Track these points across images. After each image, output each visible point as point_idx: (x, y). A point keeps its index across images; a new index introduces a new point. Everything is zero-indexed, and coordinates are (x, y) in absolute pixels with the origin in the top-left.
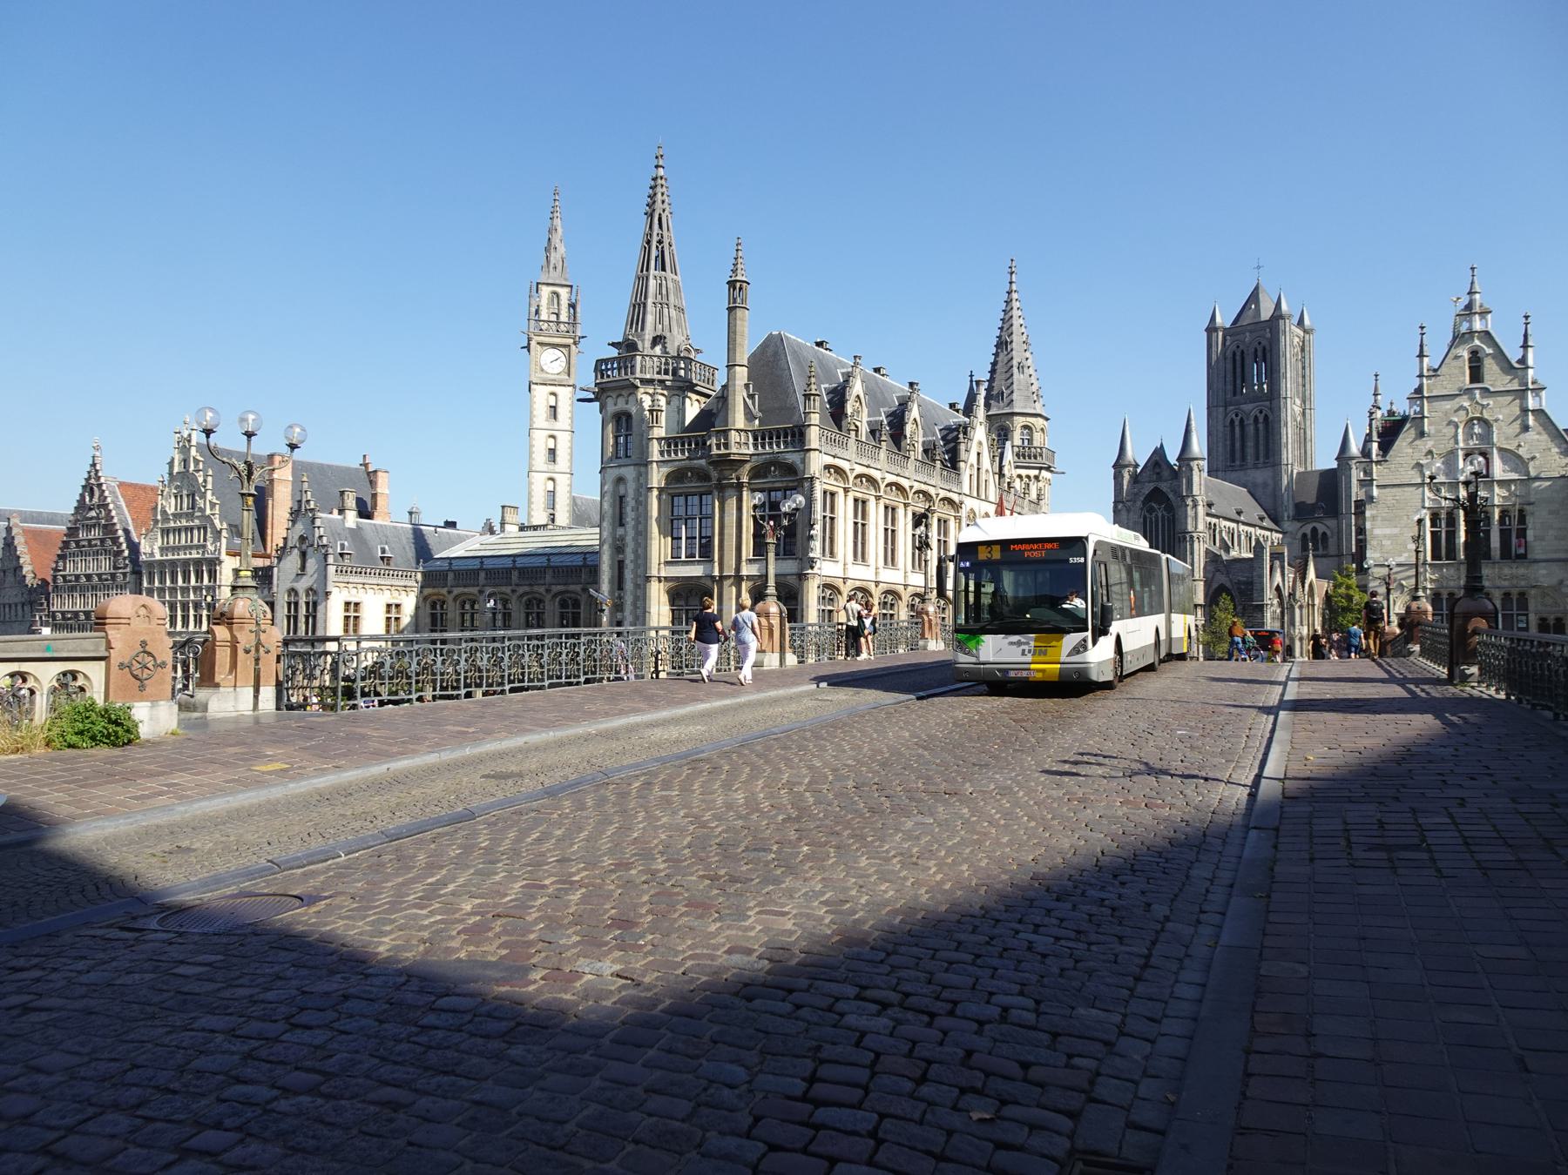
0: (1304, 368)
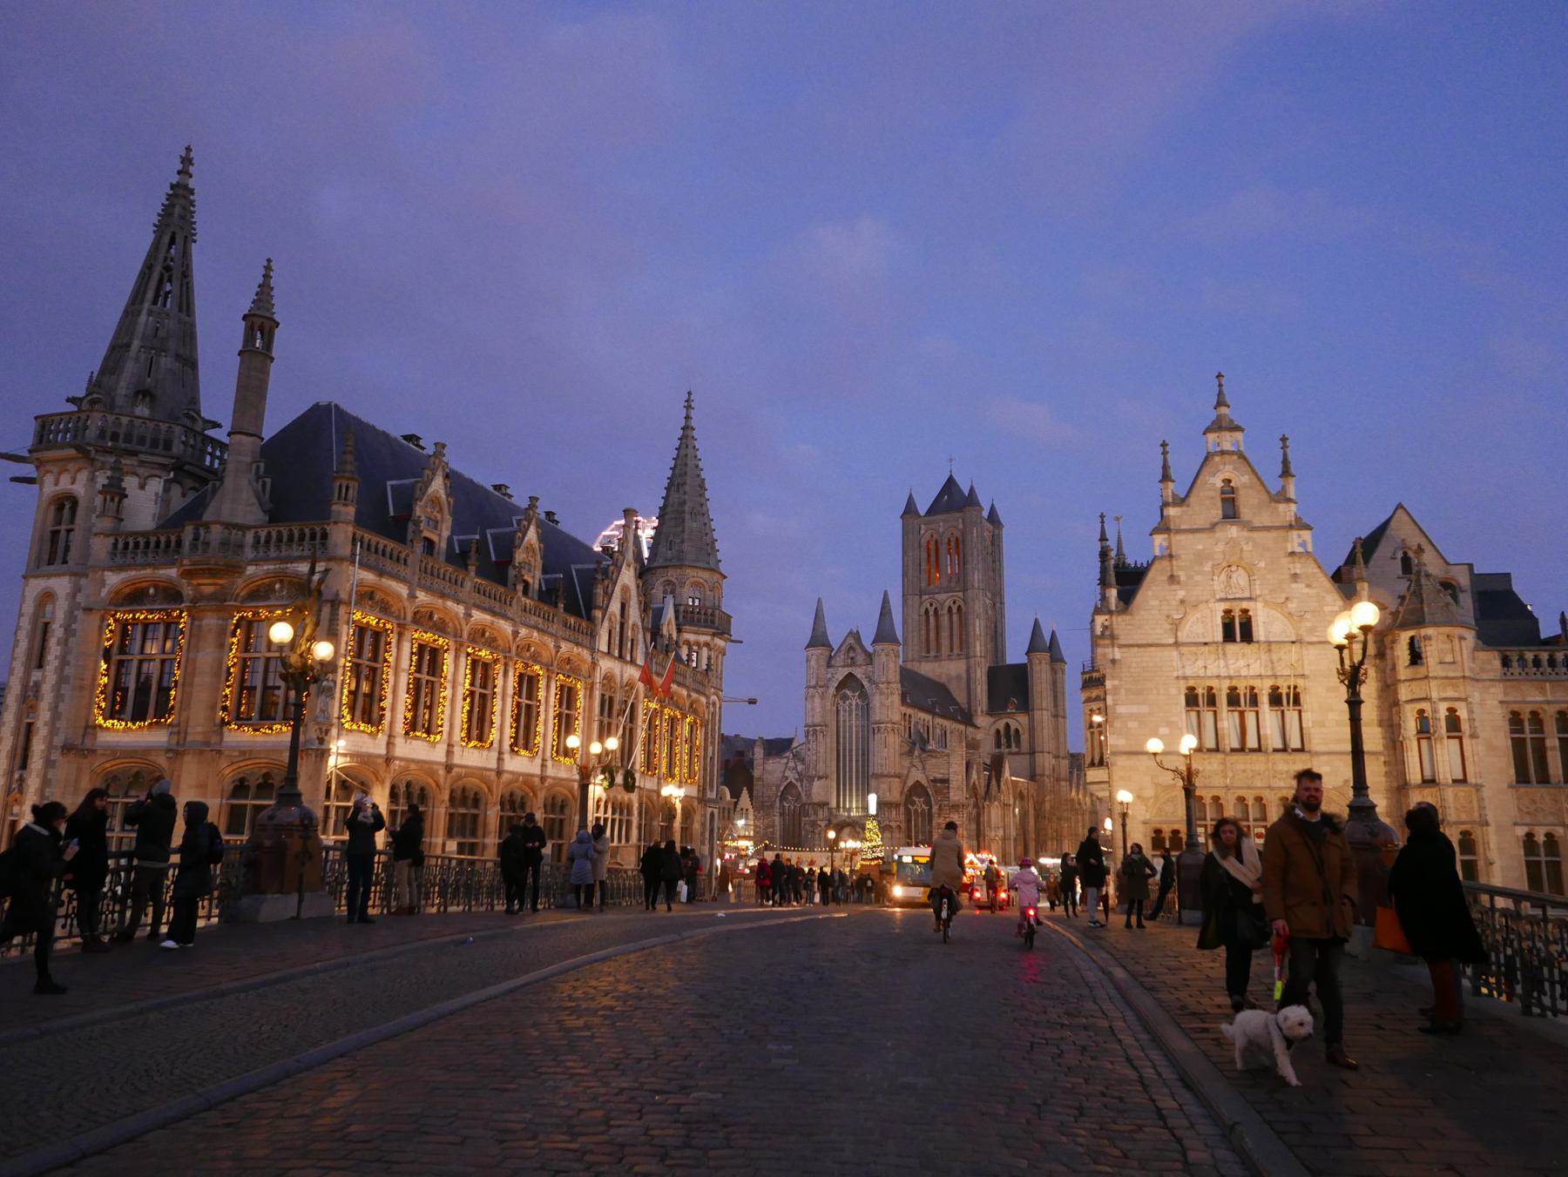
0: (994, 562)
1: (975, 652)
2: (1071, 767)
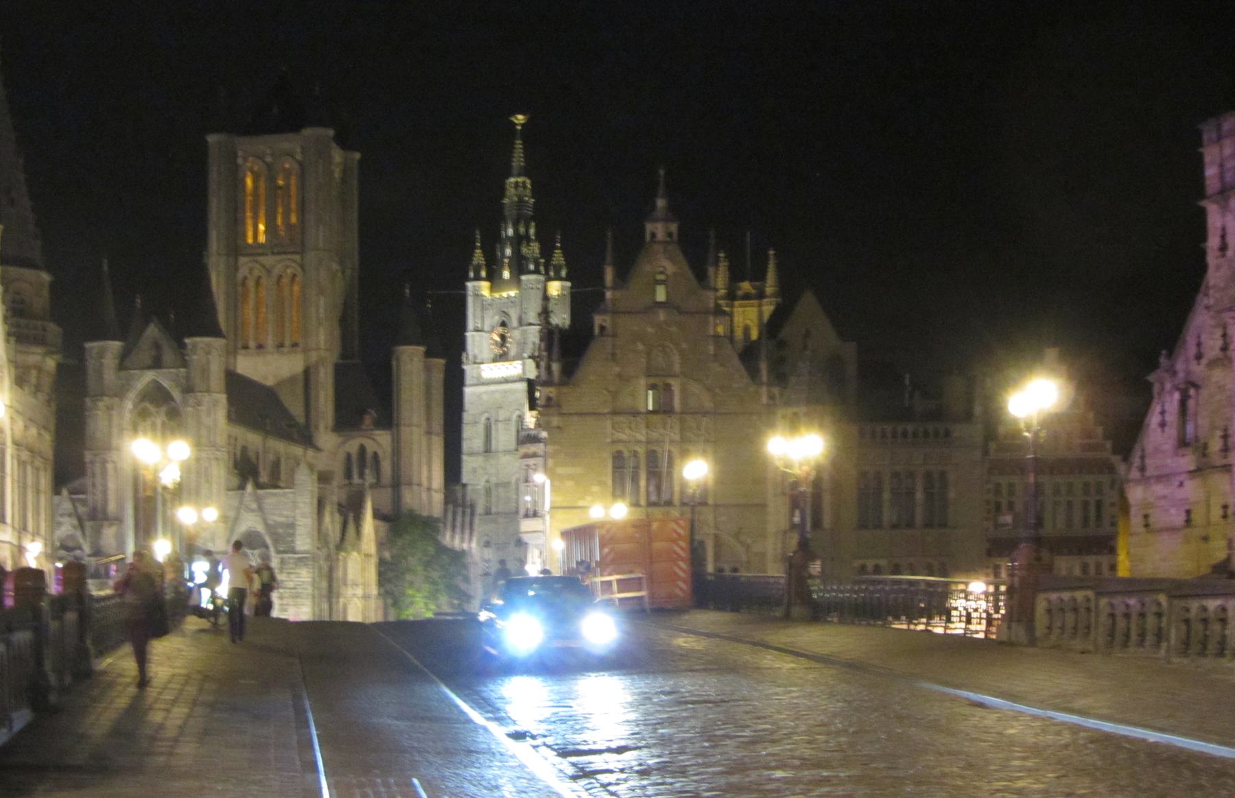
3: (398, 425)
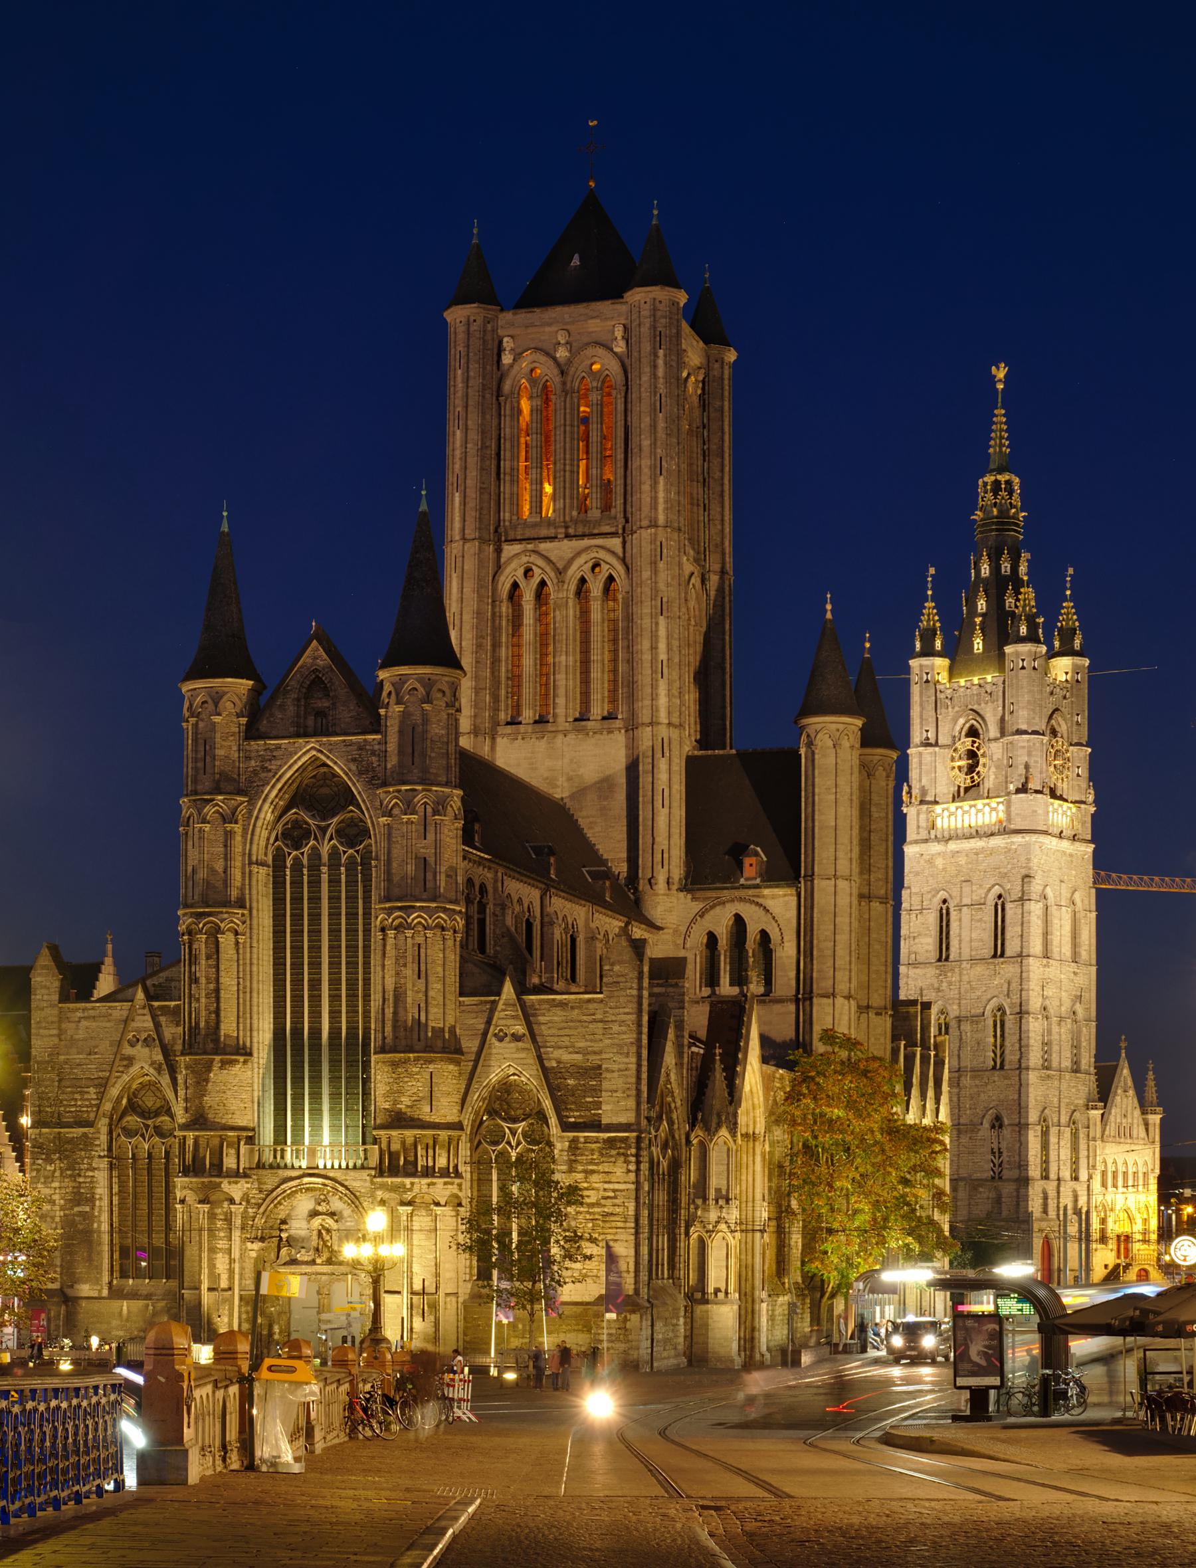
1: (654, 710)
2: (895, 1038)
3: (811, 877)
